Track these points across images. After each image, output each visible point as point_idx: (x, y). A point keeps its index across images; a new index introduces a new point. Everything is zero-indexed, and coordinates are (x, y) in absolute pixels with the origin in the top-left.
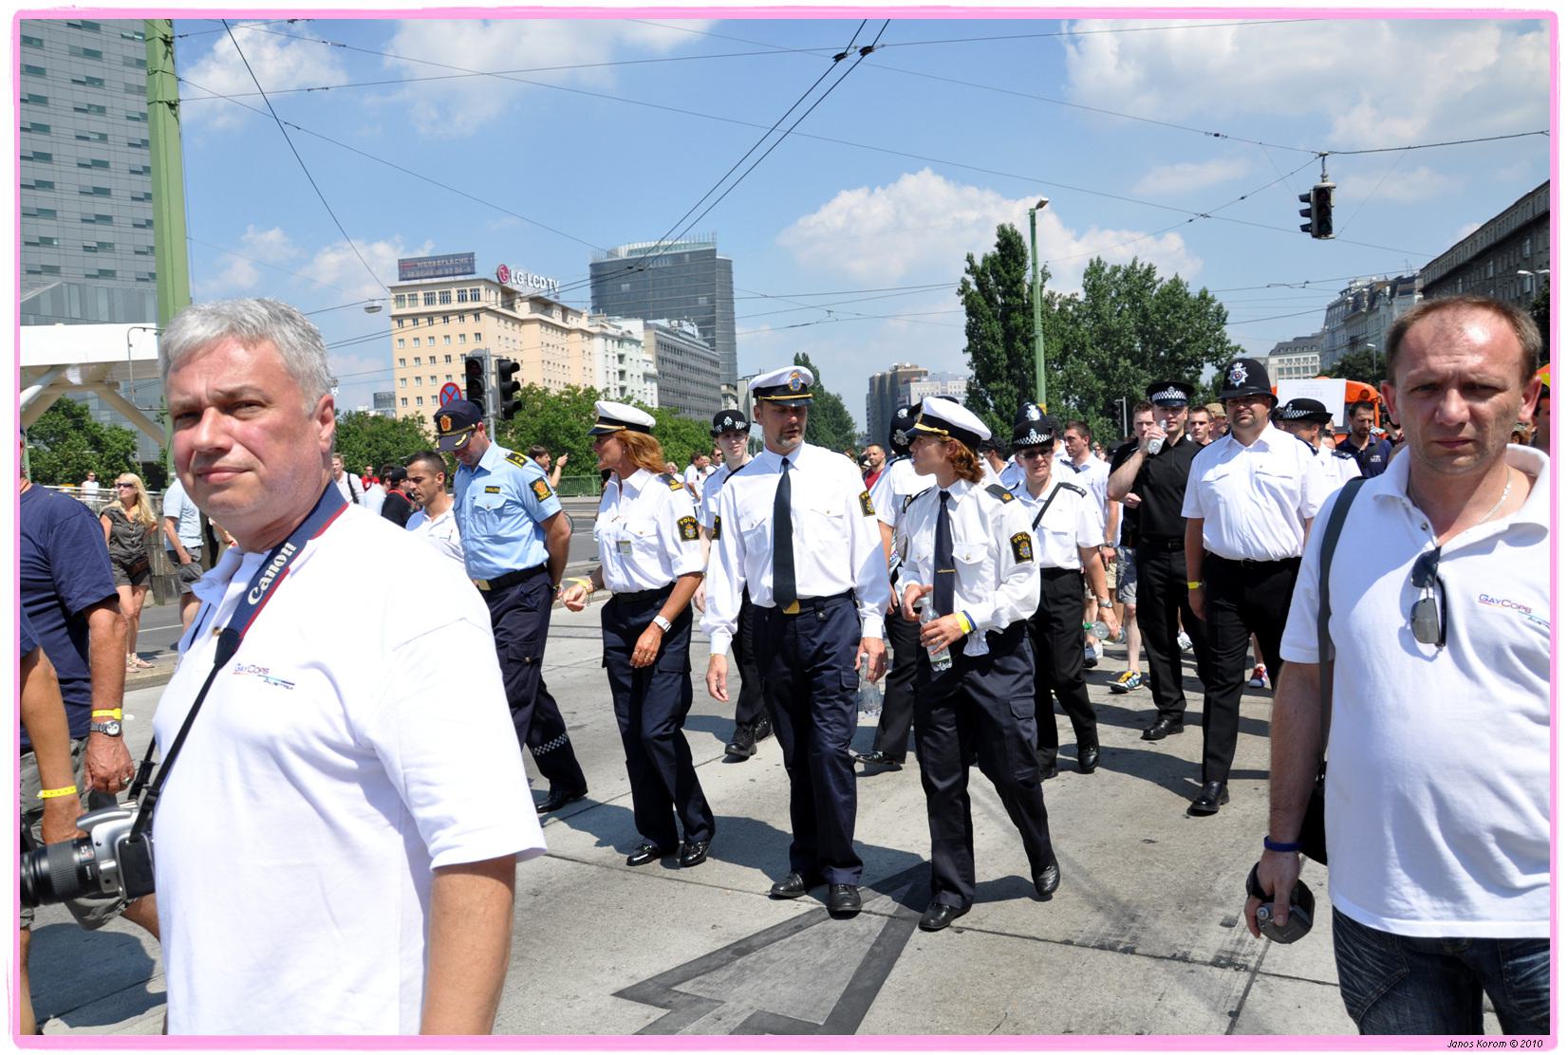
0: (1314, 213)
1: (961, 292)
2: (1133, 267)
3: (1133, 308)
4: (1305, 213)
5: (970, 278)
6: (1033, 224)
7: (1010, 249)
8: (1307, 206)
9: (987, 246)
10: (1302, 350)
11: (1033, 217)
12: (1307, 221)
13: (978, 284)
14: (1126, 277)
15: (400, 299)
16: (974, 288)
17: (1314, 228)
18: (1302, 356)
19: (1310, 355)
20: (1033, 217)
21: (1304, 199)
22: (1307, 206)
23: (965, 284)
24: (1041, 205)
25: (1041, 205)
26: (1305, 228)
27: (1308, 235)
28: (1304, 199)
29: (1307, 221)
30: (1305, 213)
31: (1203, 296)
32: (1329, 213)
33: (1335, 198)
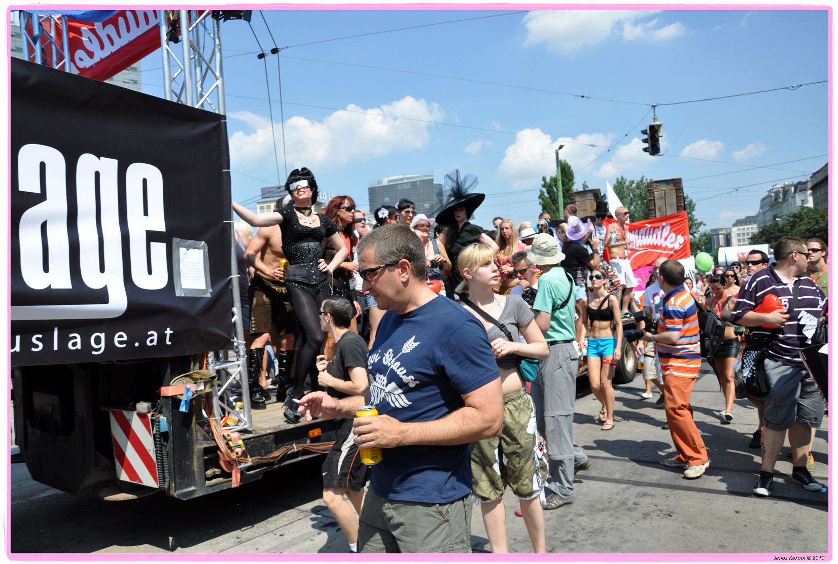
1: (540, 197)
2: (642, 181)
5: (544, 190)
7: (565, 171)
8: (646, 137)
9: (552, 171)
10: (750, 223)
11: (557, 154)
12: (646, 145)
13: (548, 193)
14: (638, 187)
15: (262, 208)
16: (546, 194)
18: (750, 227)
19: (755, 226)
20: (557, 154)
21: (644, 132)
22: (646, 137)
23: (542, 193)
24: (561, 147)
25: (561, 147)
26: (645, 150)
28: (644, 132)
29: (646, 145)
30: (645, 141)
32: (657, 140)
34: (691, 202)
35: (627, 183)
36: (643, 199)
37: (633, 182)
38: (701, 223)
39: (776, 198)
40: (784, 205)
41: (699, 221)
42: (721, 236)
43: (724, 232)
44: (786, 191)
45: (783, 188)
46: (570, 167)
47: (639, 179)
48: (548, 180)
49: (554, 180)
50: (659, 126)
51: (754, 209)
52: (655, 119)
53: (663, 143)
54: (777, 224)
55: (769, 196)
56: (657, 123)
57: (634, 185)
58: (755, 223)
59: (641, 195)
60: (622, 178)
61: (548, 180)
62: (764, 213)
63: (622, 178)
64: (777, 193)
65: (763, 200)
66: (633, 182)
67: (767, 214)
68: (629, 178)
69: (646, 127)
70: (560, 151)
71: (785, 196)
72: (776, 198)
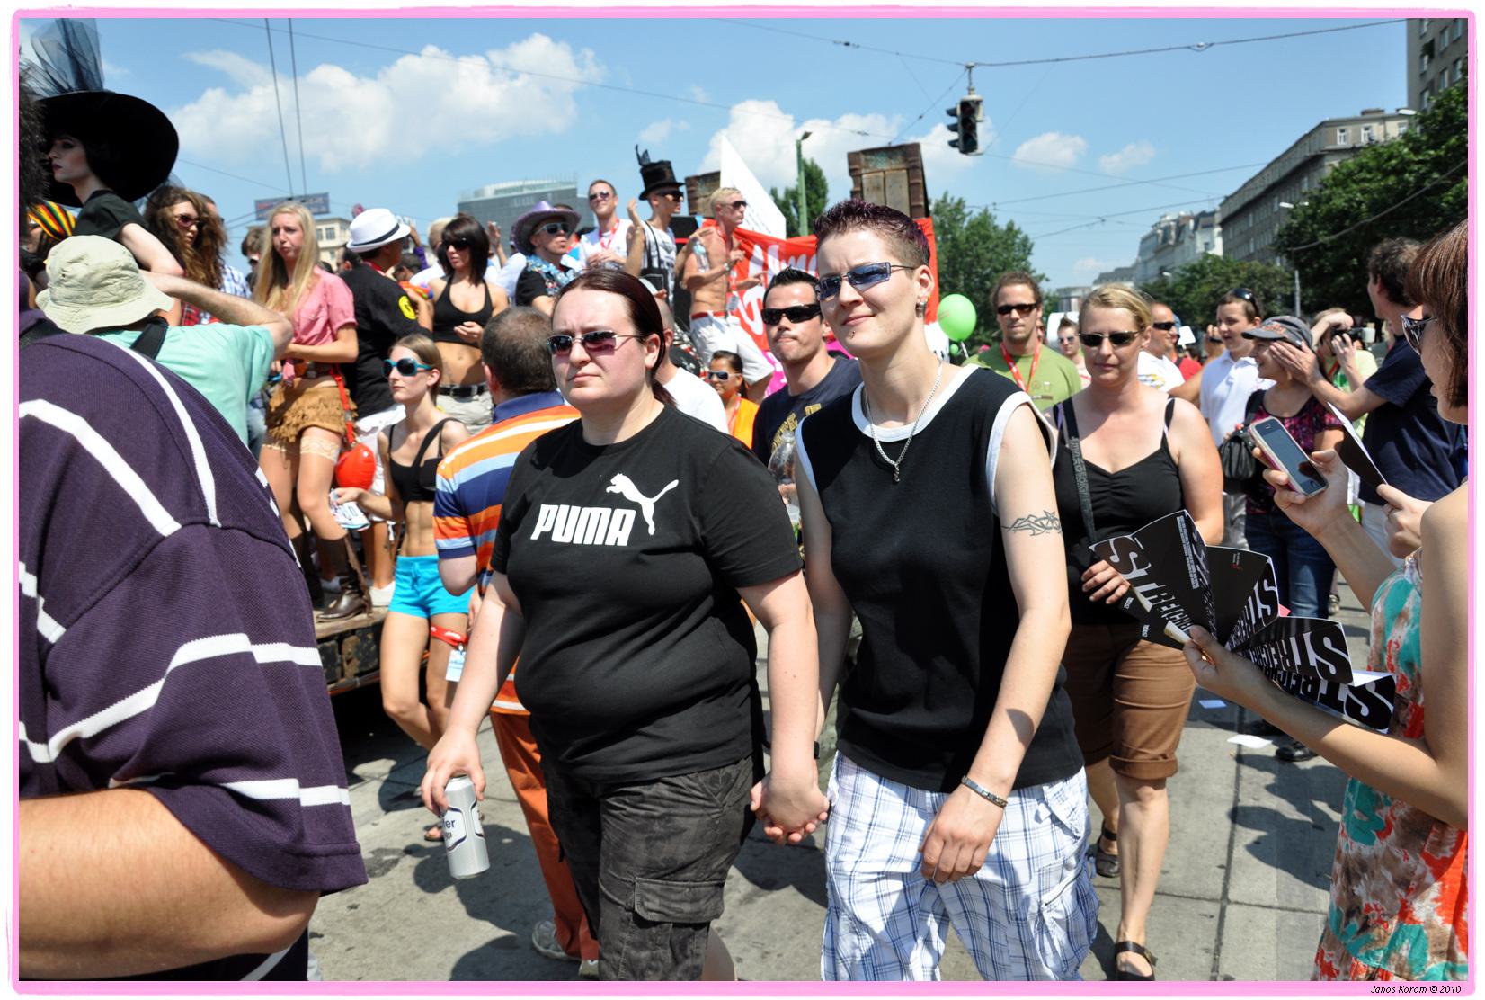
3: (944, 240)
6: (799, 155)
8: (954, 120)
11: (799, 148)
12: (955, 136)
20: (799, 148)
21: (952, 113)
22: (954, 120)
24: (806, 136)
25: (806, 136)
26: (953, 144)
27: (956, 151)
28: (952, 113)
29: (955, 136)
30: (953, 128)
31: (1010, 228)
32: (973, 127)
34: (1026, 239)
36: (945, 232)
38: (1042, 277)
39: (1165, 239)
40: (1178, 250)
41: (1039, 273)
42: (1074, 301)
43: (1079, 293)
44: (1180, 228)
45: (1177, 221)
46: (820, 173)
48: (781, 195)
49: (793, 195)
50: (978, 103)
51: (1128, 256)
52: (970, 90)
53: (983, 132)
54: (1164, 281)
55: (1154, 234)
56: (974, 97)
58: (1129, 279)
59: (941, 226)
61: (781, 195)
62: (1145, 263)
65: (1144, 240)
67: (1150, 265)
69: (955, 104)
70: (804, 143)
71: (1178, 235)
72: (1165, 239)
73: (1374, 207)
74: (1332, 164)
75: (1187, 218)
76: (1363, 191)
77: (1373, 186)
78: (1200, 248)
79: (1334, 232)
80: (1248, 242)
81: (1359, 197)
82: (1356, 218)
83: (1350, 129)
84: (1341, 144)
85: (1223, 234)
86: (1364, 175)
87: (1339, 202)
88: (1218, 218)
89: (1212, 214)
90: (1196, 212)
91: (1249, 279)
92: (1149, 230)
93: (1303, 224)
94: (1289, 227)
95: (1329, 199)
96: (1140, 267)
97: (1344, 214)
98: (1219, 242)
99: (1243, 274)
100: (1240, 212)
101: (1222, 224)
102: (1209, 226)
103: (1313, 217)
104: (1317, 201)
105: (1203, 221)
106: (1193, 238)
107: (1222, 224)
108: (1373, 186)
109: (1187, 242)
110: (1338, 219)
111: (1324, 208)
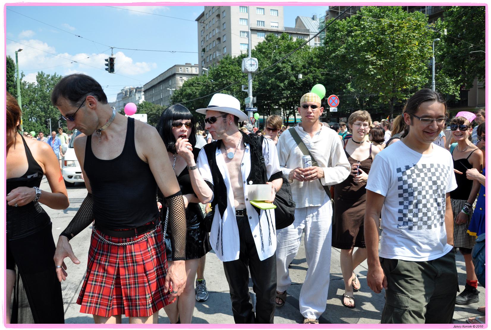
0: (109, 65)
4: (107, 65)
8: (107, 63)
12: (107, 67)
17: (109, 69)
21: (106, 60)
22: (107, 63)
26: (106, 69)
28: (106, 60)
29: (107, 67)
30: (107, 65)
32: (113, 65)
33: (115, 62)
35: (45, 76)
37: (49, 76)
39: (126, 95)
40: (130, 98)
44: (131, 92)
45: (130, 89)
47: (53, 75)
50: (114, 58)
53: (116, 67)
57: (50, 78)
60: (42, 72)
62: (119, 102)
63: (42, 72)
64: (126, 92)
65: (118, 94)
66: (49, 76)
68: (46, 73)
69: (107, 57)
71: (130, 94)
72: (126, 95)
73: (201, 94)
74: (178, 77)
75: (134, 88)
76: (197, 89)
77: (199, 88)
78: (137, 98)
79: (188, 99)
80: (152, 98)
81: (196, 91)
82: (195, 96)
83: (183, 68)
84: (180, 72)
85: (145, 95)
86: (195, 85)
87: (189, 91)
88: (143, 89)
89: (141, 88)
90: (136, 87)
91: (158, 110)
92: (120, 91)
93: (178, 96)
94: (174, 96)
95: (185, 90)
96: (117, 103)
97: (190, 95)
98: (143, 97)
99: (156, 108)
100: (150, 89)
101: (144, 92)
102: (140, 92)
103: (181, 94)
104: (182, 90)
105: (138, 90)
106: (135, 95)
107: (144, 92)
108: (199, 88)
109: (133, 96)
110: (189, 96)
111: (184, 93)
